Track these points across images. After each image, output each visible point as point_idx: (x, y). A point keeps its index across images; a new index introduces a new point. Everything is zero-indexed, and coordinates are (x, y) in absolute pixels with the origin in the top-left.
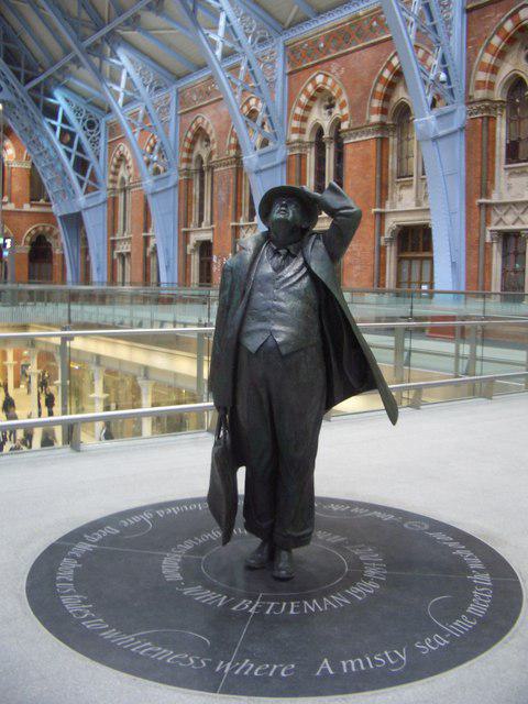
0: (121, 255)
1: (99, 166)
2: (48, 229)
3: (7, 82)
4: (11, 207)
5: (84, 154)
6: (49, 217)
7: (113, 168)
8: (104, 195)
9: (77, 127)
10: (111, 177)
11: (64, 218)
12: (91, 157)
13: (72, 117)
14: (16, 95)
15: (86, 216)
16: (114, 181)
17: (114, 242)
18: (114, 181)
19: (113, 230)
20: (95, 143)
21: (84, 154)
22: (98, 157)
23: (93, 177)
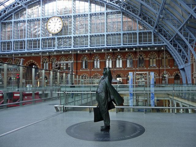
0: (194, 77)
1: (189, 57)
2: (178, 72)
3: (165, 41)
4: (169, 68)
5: (184, 54)
6: (178, 70)
7: (192, 57)
8: (189, 63)
9: (182, 48)
10: (191, 59)
11: (181, 69)
12: (186, 54)
13: (180, 46)
14: (167, 43)
15: (185, 69)
16: (192, 60)
17: (193, 74)
18: (192, 60)
19: (192, 71)
20: (187, 51)
21: (184, 54)
22: (188, 55)
23: (187, 59)
